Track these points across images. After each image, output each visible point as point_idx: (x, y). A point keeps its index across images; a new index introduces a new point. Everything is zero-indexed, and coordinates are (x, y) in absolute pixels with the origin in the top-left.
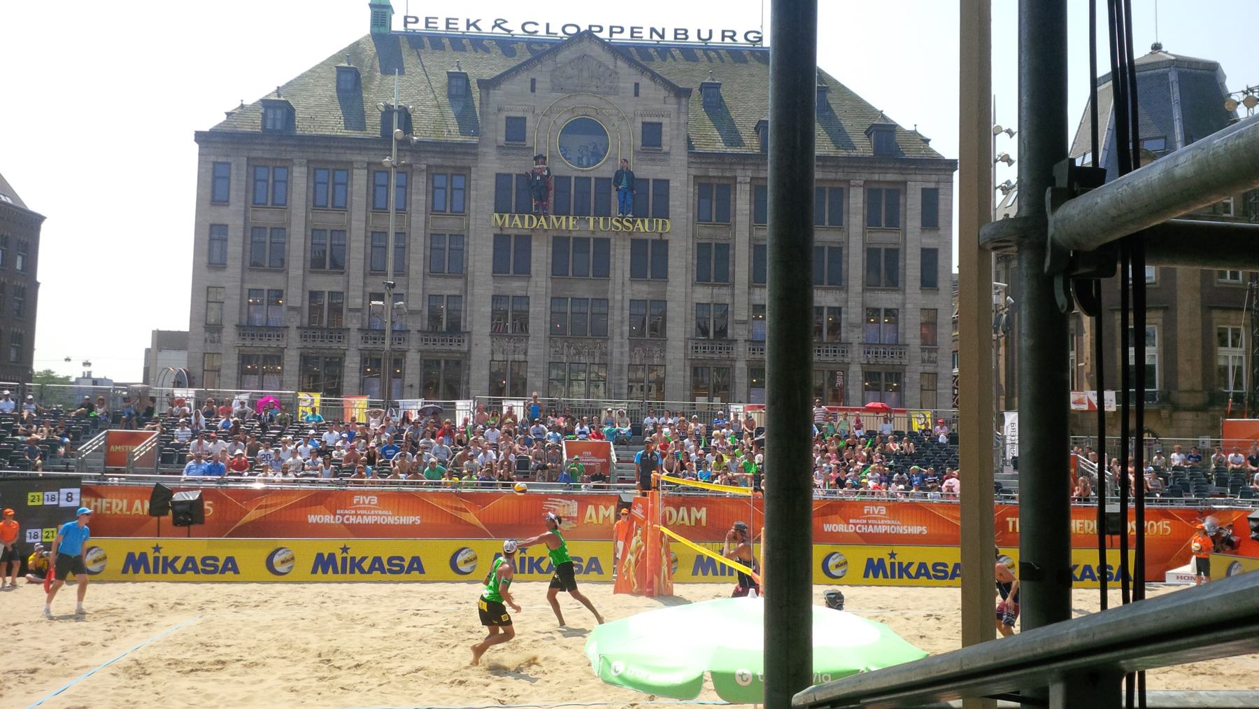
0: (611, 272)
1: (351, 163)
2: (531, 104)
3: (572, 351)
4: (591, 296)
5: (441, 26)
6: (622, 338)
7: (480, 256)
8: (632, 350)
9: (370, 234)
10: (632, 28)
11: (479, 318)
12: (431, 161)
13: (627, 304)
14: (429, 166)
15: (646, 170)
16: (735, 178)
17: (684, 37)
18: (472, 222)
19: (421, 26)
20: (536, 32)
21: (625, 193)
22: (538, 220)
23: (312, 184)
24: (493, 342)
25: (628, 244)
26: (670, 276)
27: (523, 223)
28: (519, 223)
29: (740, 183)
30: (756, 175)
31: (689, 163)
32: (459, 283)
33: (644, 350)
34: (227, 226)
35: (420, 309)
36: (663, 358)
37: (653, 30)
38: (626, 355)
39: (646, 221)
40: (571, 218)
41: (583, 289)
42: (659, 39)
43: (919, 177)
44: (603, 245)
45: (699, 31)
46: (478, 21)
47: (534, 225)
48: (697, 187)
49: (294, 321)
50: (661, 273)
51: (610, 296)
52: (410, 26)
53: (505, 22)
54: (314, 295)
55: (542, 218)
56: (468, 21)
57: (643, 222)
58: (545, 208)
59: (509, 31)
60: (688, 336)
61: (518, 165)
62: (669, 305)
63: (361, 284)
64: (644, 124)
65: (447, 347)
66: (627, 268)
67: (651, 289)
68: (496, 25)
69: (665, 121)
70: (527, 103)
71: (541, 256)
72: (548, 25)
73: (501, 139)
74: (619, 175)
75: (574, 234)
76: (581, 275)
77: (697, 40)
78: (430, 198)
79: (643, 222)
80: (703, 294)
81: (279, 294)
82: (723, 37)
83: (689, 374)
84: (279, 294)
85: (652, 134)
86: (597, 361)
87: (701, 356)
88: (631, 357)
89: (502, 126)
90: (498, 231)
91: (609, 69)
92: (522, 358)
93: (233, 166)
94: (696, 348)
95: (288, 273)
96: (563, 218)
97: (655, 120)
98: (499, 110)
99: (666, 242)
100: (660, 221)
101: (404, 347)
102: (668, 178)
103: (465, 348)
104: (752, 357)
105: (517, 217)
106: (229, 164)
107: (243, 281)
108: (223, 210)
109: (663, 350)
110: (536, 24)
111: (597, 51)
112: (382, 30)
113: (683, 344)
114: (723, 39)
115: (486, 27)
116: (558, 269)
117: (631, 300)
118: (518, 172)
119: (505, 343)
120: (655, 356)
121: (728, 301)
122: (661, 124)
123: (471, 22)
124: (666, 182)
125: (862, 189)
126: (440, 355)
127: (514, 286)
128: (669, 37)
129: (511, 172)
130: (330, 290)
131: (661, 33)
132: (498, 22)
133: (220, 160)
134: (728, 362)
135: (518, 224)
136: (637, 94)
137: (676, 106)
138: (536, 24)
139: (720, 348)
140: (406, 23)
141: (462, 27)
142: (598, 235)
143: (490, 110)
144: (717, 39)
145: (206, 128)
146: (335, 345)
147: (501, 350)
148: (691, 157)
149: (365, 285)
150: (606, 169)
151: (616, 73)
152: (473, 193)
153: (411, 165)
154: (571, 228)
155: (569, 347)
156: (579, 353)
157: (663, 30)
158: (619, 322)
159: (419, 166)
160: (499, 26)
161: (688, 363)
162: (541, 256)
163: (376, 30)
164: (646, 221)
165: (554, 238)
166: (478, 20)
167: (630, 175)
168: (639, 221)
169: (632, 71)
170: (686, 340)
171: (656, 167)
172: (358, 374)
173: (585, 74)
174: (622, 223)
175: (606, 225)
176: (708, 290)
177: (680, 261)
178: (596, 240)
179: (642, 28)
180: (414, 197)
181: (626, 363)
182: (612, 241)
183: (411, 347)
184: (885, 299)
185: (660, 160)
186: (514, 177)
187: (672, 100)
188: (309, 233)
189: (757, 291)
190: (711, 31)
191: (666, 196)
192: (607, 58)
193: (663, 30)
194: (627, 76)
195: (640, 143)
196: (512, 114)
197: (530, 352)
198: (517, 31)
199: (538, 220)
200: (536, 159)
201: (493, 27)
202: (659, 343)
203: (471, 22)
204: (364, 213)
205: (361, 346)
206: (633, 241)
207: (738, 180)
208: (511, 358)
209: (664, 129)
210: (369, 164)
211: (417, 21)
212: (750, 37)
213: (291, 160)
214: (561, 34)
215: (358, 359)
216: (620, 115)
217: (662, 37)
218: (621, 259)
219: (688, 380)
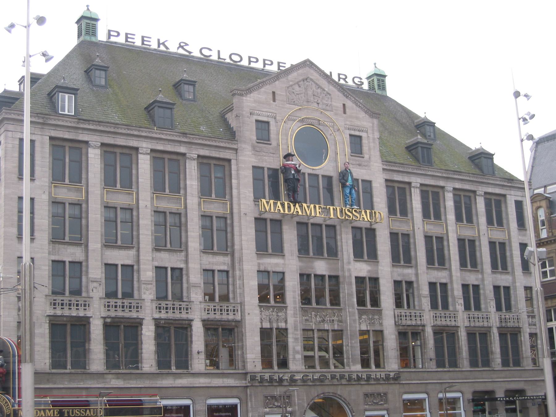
0: (339, 253)
1: (137, 149)
2: (274, 111)
3: (318, 319)
8: (360, 318)
13: (354, 281)
15: (358, 173)
18: (235, 206)
19: (121, 40)
20: (210, 56)
22: (295, 206)
24: (261, 311)
25: (350, 230)
26: (380, 258)
28: (281, 208)
29: (414, 187)
30: (423, 182)
31: (384, 169)
32: (228, 259)
33: (369, 319)
36: (381, 324)
39: (368, 211)
40: (317, 206)
43: (512, 192)
46: (166, 41)
52: (113, 39)
53: (187, 45)
56: (159, 40)
57: (366, 212)
58: (300, 197)
59: (190, 53)
63: (151, 258)
64: (351, 135)
68: (180, 46)
69: (364, 135)
70: (271, 111)
72: (219, 52)
75: (312, 221)
76: (319, 253)
79: (366, 212)
88: (360, 323)
89: (253, 126)
90: (257, 216)
91: (324, 90)
92: (282, 325)
95: (87, 246)
97: (357, 133)
101: (190, 317)
102: (371, 180)
109: (380, 318)
110: (210, 50)
112: (93, 39)
115: (173, 48)
116: (303, 249)
117: (356, 278)
118: (269, 166)
121: (413, 279)
123: (161, 42)
124: (370, 182)
125: (483, 198)
129: (263, 166)
130: (122, 263)
132: (182, 44)
134: (421, 328)
136: (345, 112)
138: (210, 50)
140: (109, 36)
141: (154, 46)
142: (328, 222)
143: (244, 113)
147: (268, 319)
151: (330, 95)
152: (234, 181)
154: (318, 215)
155: (316, 316)
156: (323, 321)
159: (192, 155)
160: (180, 46)
164: (368, 211)
165: (298, 223)
166: (166, 41)
168: (363, 213)
171: (362, 171)
173: (310, 93)
174: (352, 213)
178: (327, 226)
180: (188, 182)
182: (338, 228)
183: (196, 317)
184: (503, 280)
186: (266, 169)
196: (260, 118)
197: (291, 320)
198: (196, 54)
199: (295, 206)
201: (178, 48)
203: (161, 42)
205: (157, 316)
207: (413, 185)
208: (275, 326)
211: (119, 34)
212: (356, 80)
214: (228, 60)
215: (153, 328)
216: (335, 127)
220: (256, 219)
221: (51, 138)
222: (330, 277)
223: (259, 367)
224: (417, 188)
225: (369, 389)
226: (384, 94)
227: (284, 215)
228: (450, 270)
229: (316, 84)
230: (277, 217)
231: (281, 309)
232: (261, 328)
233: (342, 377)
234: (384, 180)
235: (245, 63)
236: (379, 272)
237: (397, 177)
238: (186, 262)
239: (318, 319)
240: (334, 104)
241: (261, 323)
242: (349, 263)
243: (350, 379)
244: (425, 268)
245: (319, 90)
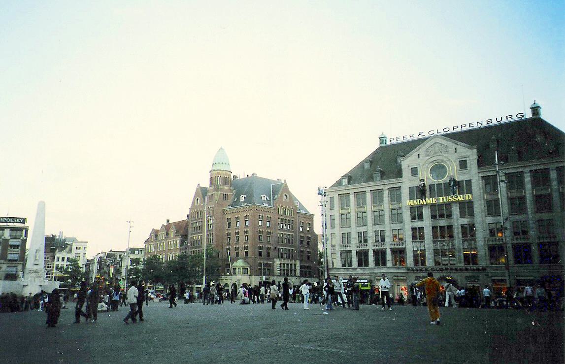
3: (441, 245)
7: (407, 215)
11: (408, 235)
12: (389, 187)
13: (460, 227)
39: (461, 196)
40: (434, 199)
41: (442, 222)
47: (421, 203)
50: (472, 214)
55: (424, 200)
61: (416, 183)
66: (459, 213)
69: (467, 159)
71: (426, 213)
74: (450, 181)
75: (438, 204)
80: (490, 220)
86: (451, 247)
87: (491, 243)
88: (463, 245)
92: (423, 248)
96: (431, 199)
97: (464, 159)
98: (409, 166)
99: (473, 202)
100: (467, 195)
103: (404, 246)
105: (415, 201)
108: (332, 211)
112: (383, 145)
122: (466, 160)
127: (418, 224)
135: (417, 202)
144: (504, 120)
150: (446, 179)
156: (444, 245)
158: (457, 232)
162: (426, 213)
163: (381, 145)
165: (431, 206)
167: (454, 181)
170: (485, 238)
173: (437, 149)
175: (446, 200)
177: (479, 208)
181: (462, 248)
191: (471, 186)
192: (445, 142)
204: (370, 206)
212: (518, 116)
218: (456, 210)
219: (487, 253)
220: (411, 208)
222: (448, 226)
223: (412, 265)
225: (468, 274)
226: (537, 117)
228: (527, 214)
231: (421, 242)
232: (414, 250)
238: (385, 228)
239: (441, 245)
242: (458, 219)
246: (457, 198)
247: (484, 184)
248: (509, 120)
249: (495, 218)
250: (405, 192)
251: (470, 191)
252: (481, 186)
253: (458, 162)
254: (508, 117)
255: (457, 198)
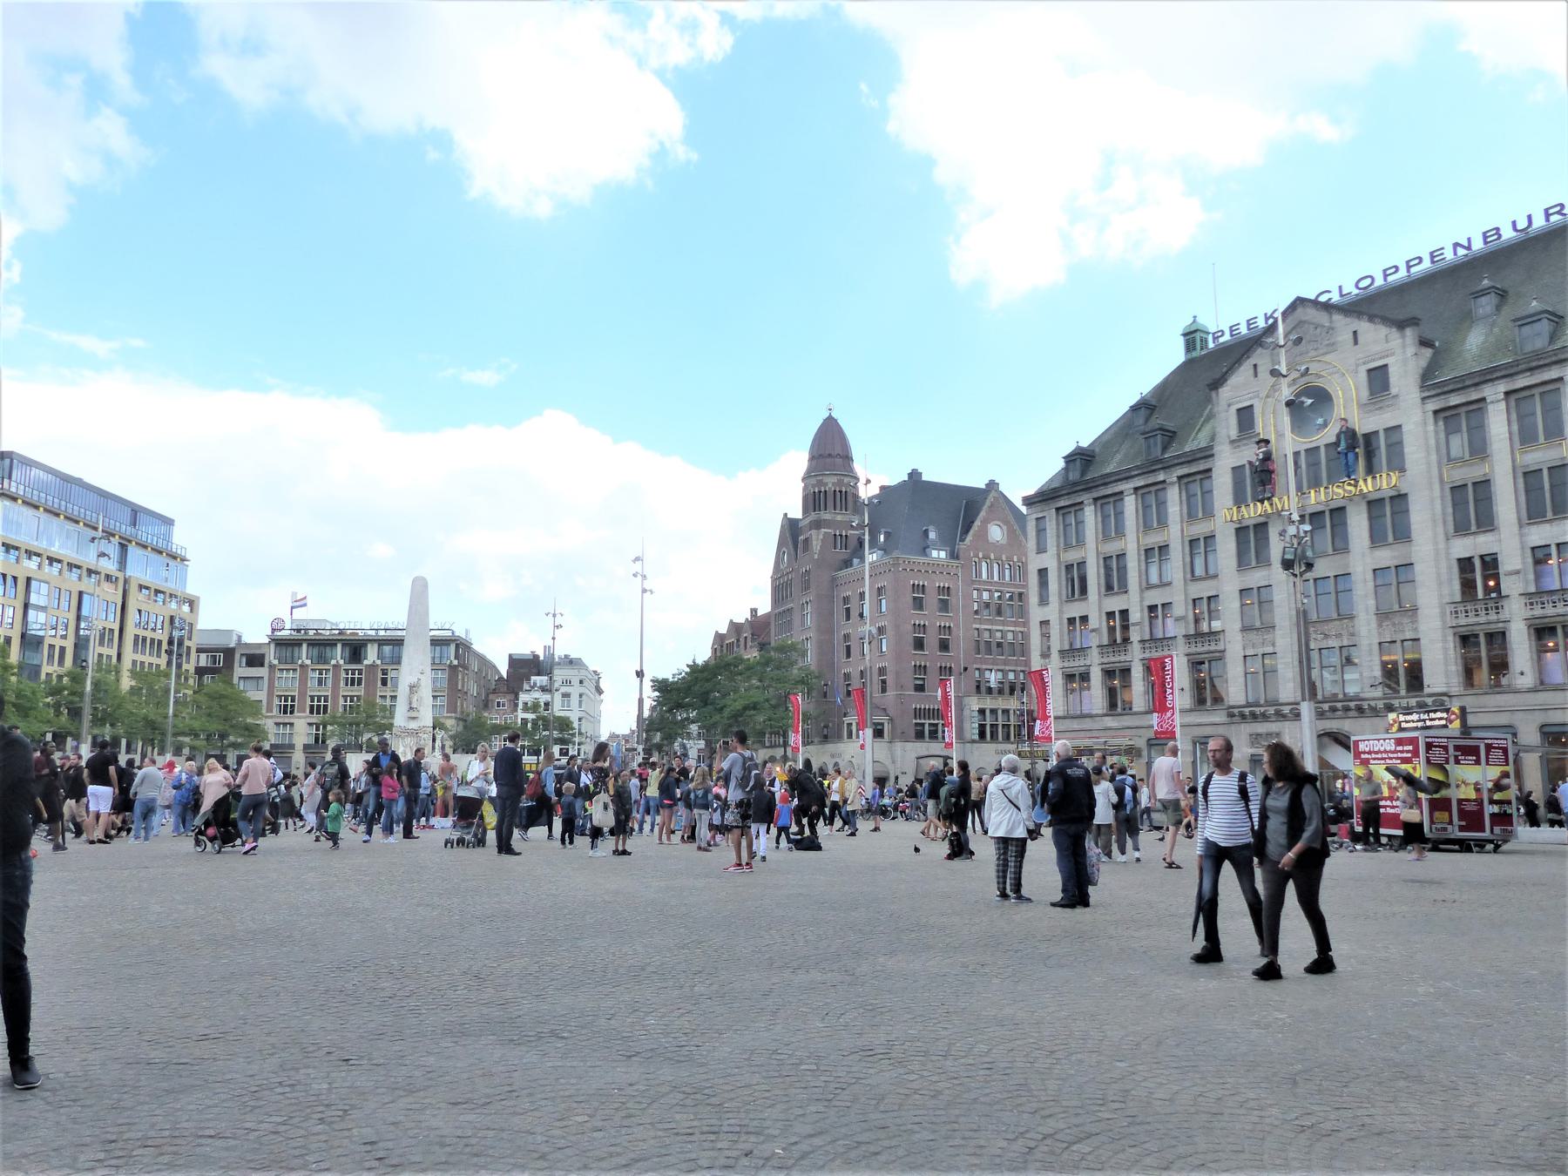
1: (1122, 492)
4: (1331, 574)
5: (1244, 330)
6: (1367, 614)
8: (1380, 625)
9: (1143, 552)
10: (1431, 253)
13: (1370, 575)
14: (1180, 478)
16: (1483, 399)
17: (1496, 237)
19: (1227, 337)
20: (1330, 299)
21: (1346, 454)
23: (1100, 519)
25: (1364, 508)
27: (1249, 514)
29: (1492, 402)
31: (1424, 399)
33: (1394, 624)
34: (1046, 569)
35: (1184, 614)
36: (1416, 630)
37: (1456, 245)
38: (1375, 632)
42: (1465, 252)
44: (1338, 513)
45: (1514, 223)
48: (1441, 423)
49: (1094, 641)
50: (1403, 534)
51: (1350, 570)
52: (1222, 340)
54: (1110, 615)
57: (1365, 480)
60: (1444, 601)
61: (1251, 454)
62: (1417, 568)
64: (1369, 371)
65: (1206, 648)
67: (1396, 554)
72: (1340, 287)
73: (1234, 432)
74: (1338, 436)
77: (1515, 234)
78: (1185, 507)
79: (1365, 480)
81: (1084, 619)
82: (1547, 215)
83: (1452, 645)
84: (1084, 619)
85: (1378, 378)
87: (1463, 621)
88: (1380, 634)
92: (1269, 649)
93: (1047, 519)
94: (1456, 612)
98: (1229, 405)
103: (1221, 647)
104: (1531, 613)
106: (1044, 517)
107: (1061, 612)
110: (1329, 292)
111: (1311, 314)
112: (1195, 354)
113: (1437, 610)
114: (1547, 220)
119: (1253, 636)
120: (1406, 629)
126: (1203, 656)
128: (1478, 245)
131: (1466, 245)
133: (1040, 515)
134: (1501, 625)
136: (1356, 342)
137: (1400, 341)
138: (1329, 292)
139: (1487, 609)
140: (1215, 339)
142: (1334, 505)
145: (1031, 491)
146: (1122, 658)
148: (1423, 391)
149: (1142, 600)
151: (1333, 329)
153: (1164, 481)
156: (1326, 636)
157: (1469, 239)
161: (1451, 631)
163: (1189, 356)
169: (1348, 320)
170: (1442, 607)
172: (1142, 683)
174: (1345, 490)
176: (1468, 541)
179: (1442, 248)
185: (1388, 406)
187: (1394, 333)
188: (1102, 562)
189: (1534, 529)
190: (1529, 217)
192: (1322, 318)
193: (1469, 239)
194: (1343, 326)
195: (1365, 393)
197: (1277, 644)
200: (1258, 443)
202: (1410, 613)
205: (1141, 657)
206: (1370, 503)
209: (1391, 370)
210: (1136, 489)
213: (1082, 502)
214: (1356, 291)
217: (1469, 248)
218: (1358, 524)
219: (1452, 652)
220: (1238, 530)
221: (1058, 509)
224: (1499, 401)
227: (1267, 516)
229: (1313, 324)
230: (1262, 520)
232: (1245, 657)
233: (1334, 710)
234: (1430, 414)
235: (1379, 282)
236: (1413, 555)
237: (1455, 400)
240: (1340, 339)
241: (1244, 649)
243: (1360, 709)
244: (1516, 528)
245: (1318, 330)
246: (1356, 486)
247: (1442, 435)
248: (1554, 218)
249: (1481, 539)
250: (1222, 483)
251: (1397, 463)
252: (1432, 442)
253: (1363, 376)
254: (1551, 211)
255: (1356, 486)
